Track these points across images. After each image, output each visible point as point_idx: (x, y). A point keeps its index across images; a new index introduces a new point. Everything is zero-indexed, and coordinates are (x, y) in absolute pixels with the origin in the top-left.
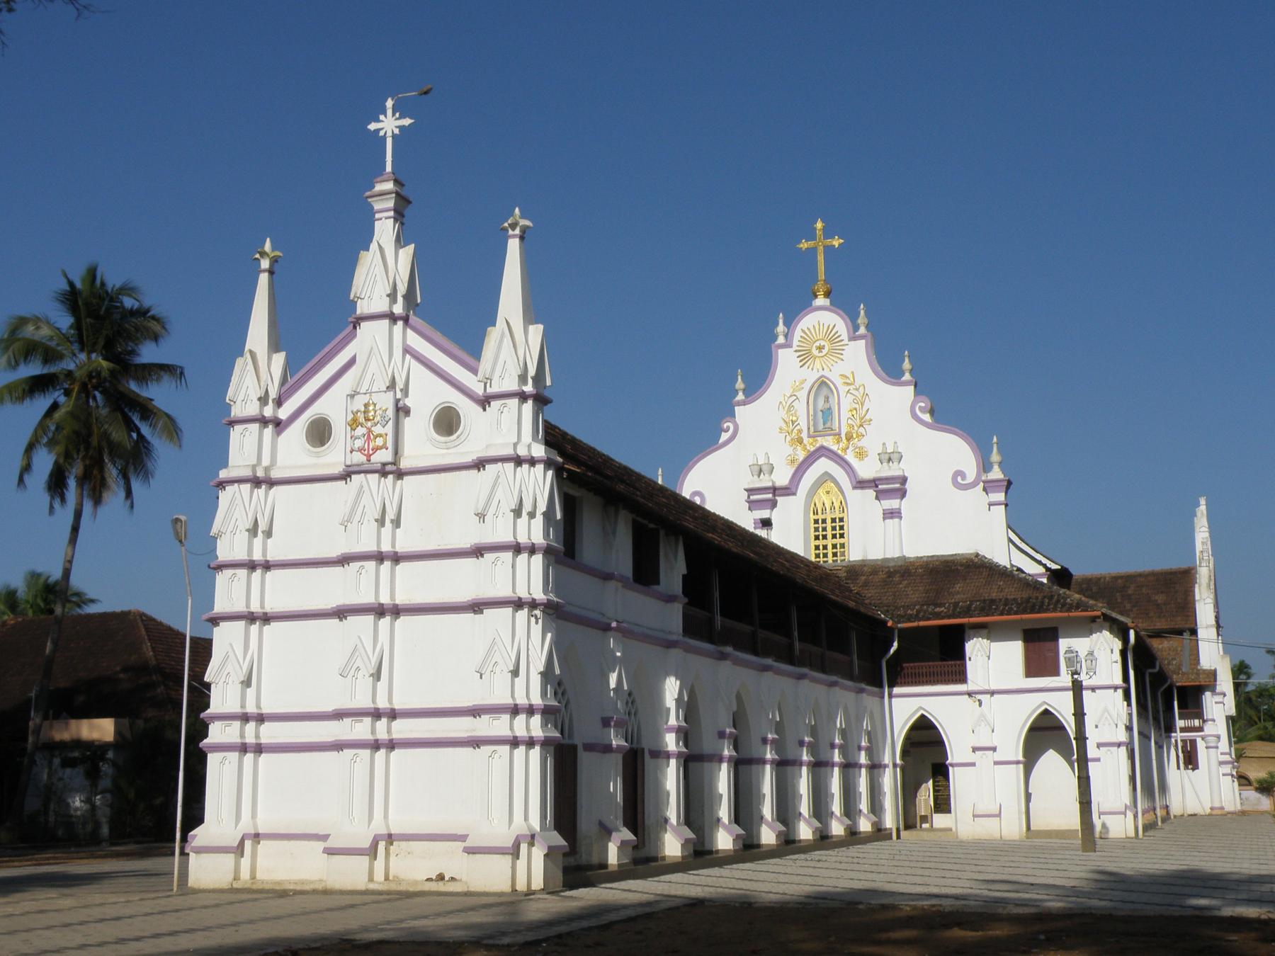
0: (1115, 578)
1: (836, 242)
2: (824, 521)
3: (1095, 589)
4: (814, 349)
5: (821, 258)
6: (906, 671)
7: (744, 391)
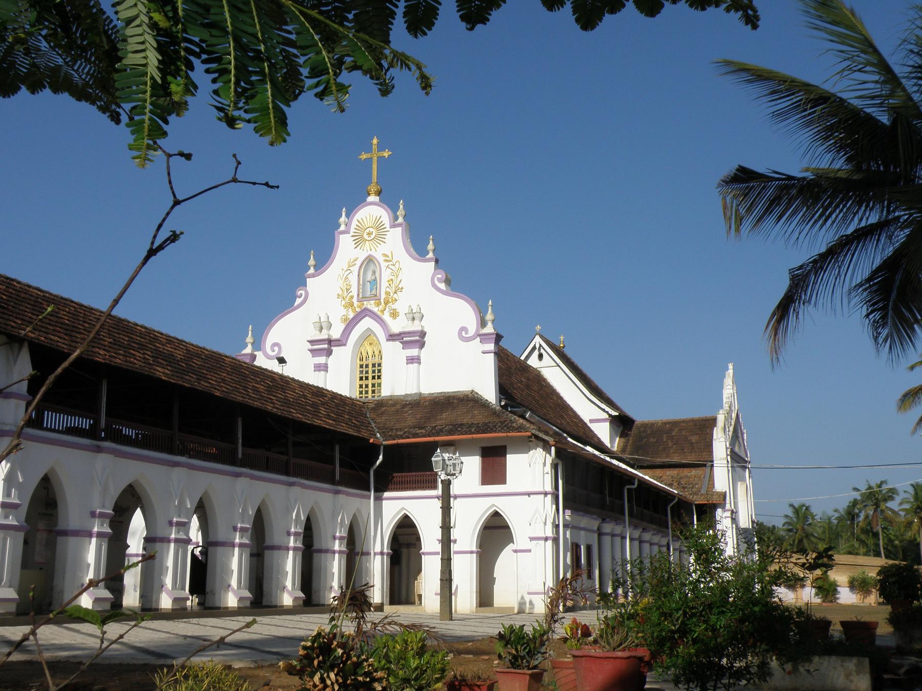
0: (665, 423)
1: (386, 154)
2: (367, 366)
3: (649, 432)
4: (365, 234)
6: (395, 479)
7: (315, 266)
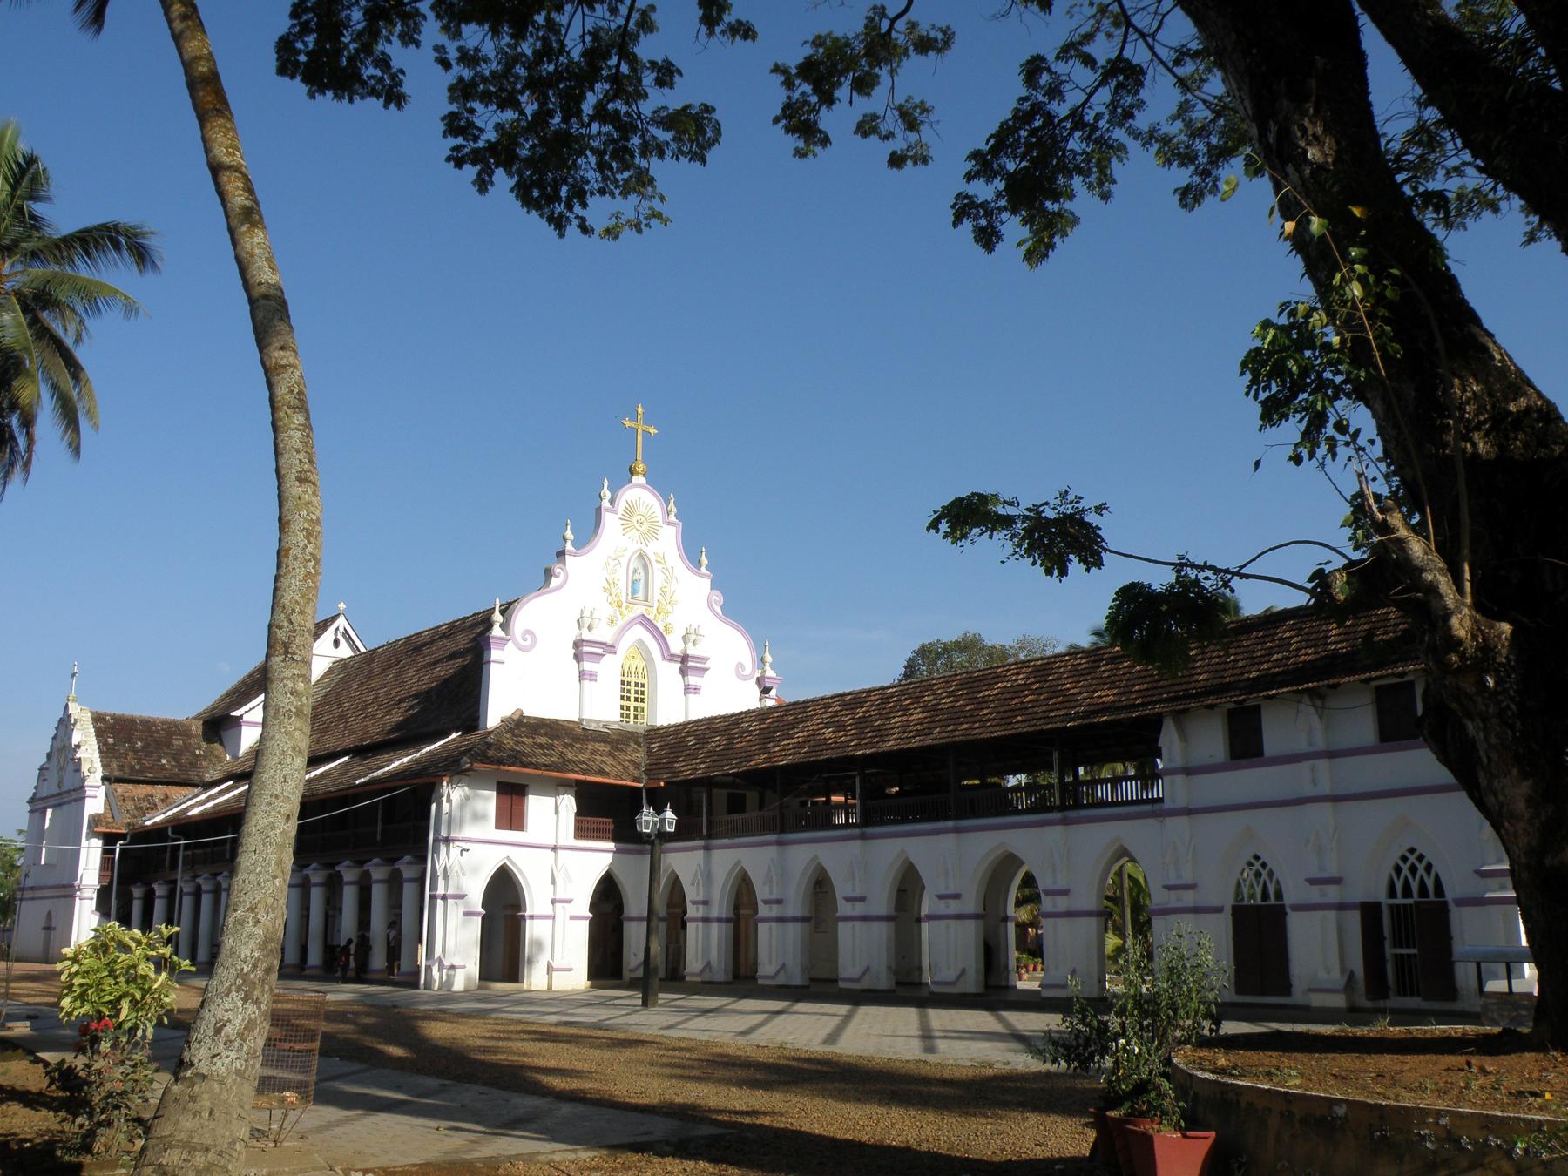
5: (640, 439)
